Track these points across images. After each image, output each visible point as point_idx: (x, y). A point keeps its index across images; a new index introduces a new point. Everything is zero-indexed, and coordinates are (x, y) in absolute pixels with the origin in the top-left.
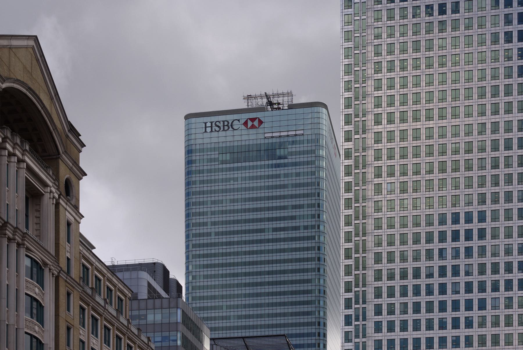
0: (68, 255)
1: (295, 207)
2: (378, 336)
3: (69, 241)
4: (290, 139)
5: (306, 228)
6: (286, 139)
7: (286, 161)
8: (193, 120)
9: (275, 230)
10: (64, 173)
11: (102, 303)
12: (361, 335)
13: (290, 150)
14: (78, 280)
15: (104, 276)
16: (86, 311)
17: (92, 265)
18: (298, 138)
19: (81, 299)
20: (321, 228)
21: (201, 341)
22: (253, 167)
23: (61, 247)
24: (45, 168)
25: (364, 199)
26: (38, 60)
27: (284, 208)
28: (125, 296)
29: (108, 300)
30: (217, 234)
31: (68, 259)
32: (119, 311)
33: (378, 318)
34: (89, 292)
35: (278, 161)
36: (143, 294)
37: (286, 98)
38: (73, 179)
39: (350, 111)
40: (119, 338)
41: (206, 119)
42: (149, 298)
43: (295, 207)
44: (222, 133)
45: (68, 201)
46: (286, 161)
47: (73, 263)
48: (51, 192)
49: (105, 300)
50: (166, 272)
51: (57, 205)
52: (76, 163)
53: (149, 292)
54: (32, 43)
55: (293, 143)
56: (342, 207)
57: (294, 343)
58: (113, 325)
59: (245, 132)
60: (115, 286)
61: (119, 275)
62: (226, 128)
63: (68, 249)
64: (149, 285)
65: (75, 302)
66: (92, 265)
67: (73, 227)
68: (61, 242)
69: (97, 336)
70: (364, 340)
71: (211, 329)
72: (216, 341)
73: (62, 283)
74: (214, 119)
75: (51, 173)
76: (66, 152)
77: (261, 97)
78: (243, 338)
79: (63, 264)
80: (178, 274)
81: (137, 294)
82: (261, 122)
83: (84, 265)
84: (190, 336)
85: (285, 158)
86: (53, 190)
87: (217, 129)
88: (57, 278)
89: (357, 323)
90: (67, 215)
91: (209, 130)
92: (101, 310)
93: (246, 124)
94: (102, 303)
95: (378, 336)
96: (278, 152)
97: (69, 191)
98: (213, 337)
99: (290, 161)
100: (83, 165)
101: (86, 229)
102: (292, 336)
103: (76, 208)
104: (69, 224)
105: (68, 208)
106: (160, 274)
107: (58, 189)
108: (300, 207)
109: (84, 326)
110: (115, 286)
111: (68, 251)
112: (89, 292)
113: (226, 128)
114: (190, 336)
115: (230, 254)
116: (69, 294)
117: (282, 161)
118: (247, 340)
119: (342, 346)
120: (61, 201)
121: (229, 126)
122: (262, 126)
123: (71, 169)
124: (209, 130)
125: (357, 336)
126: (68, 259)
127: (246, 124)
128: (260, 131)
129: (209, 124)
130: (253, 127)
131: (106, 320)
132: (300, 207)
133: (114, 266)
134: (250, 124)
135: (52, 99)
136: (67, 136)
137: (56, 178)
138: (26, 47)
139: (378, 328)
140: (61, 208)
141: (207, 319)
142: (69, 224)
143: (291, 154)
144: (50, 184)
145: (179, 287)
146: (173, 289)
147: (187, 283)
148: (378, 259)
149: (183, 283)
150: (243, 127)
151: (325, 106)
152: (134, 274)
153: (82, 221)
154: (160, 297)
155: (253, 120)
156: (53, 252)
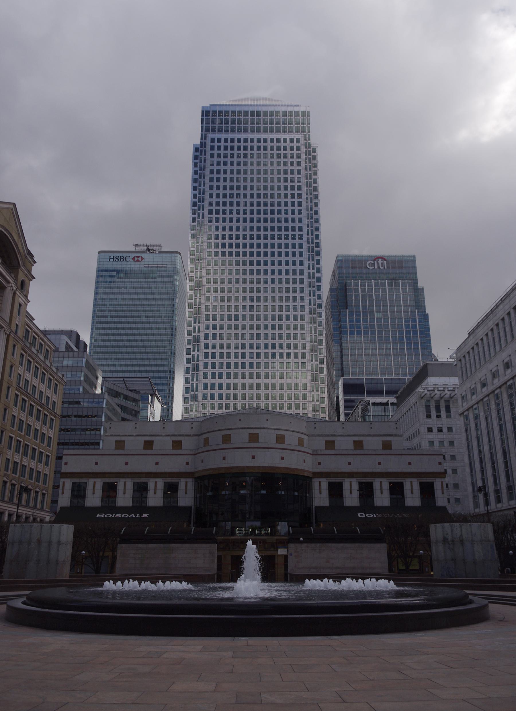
0: (17, 323)
1: (159, 305)
2: (206, 381)
3: (19, 315)
4: (159, 269)
5: (165, 317)
6: (156, 269)
7: (156, 280)
8: (103, 254)
9: (147, 317)
10: (21, 277)
11: (36, 352)
12: (195, 379)
13: (158, 274)
14: (21, 338)
15: (39, 336)
16: (25, 356)
17: (31, 329)
18: (163, 269)
19: (22, 349)
20: (174, 317)
21: (96, 378)
22: (136, 282)
23: (13, 318)
24: (10, 273)
25: (200, 304)
26: (14, 216)
27: (153, 305)
28: (51, 349)
29: (40, 350)
30: (112, 317)
31: (17, 325)
32: (46, 357)
33: (206, 370)
34: (28, 345)
35: (151, 280)
36: (63, 348)
37: (157, 248)
38: (27, 280)
39: (194, 257)
40: (44, 374)
41: (110, 254)
42: (66, 351)
43: (159, 305)
44: (119, 263)
45: (22, 292)
46: (156, 280)
47: (20, 327)
48: (11, 286)
49: (38, 351)
50: (78, 336)
51: (14, 294)
52: (29, 272)
53: (66, 348)
54: (12, 206)
55: (160, 271)
56: (187, 307)
57: (154, 382)
58: (41, 366)
59: (133, 263)
60: (45, 343)
61: (49, 336)
62: (122, 260)
63: (18, 319)
64: (67, 343)
65: (18, 351)
66: (31, 329)
67: (22, 307)
68: (14, 315)
69: (29, 372)
70: (197, 382)
71: (103, 371)
72: (106, 379)
73: (11, 339)
74: (115, 255)
75: (13, 276)
76: (24, 265)
77: (144, 246)
78: (123, 378)
79: (13, 328)
80: (86, 337)
81: (58, 348)
82: (142, 259)
83: (26, 329)
84: (89, 375)
85: (155, 278)
86: (13, 285)
87: (117, 260)
88: (8, 336)
89: (193, 372)
90: (20, 299)
91: (112, 260)
92: (34, 357)
93: (133, 259)
94: (36, 352)
95: (206, 381)
96: (151, 275)
97: (23, 286)
98: (104, 376)
99: (158, 280)
100: (33, 273)
101: (30, 309)
102: (153, 378)
103: (26, 296)
104: (20, 305)
105: (21, 296)
106: (74, 338)
107: (16, 285)
108: (163, 305)
109: (22, 365)
110: (45, 343)
111: (17, 320)
112: (28, 345)
113: (122, 260)
114: (89, 375)
115: (119, 329)
116: (14, 346)
117: (153, 280)
118: (125, 379)
119: (184, 386)
120: (17, 292)
121: (123, 259)
122: (143, 260)
123: (26, 275)
124: (112, 260)
125: (193, 380)
126: (17, 325)
127: (133, 259)
128: (142, 263)
129: (112, 257)
130: (138, 261)
131: (37, 362)
132: (163, 305)
133: (46, 331)
134: (136, 259)
135: (19, 236)
136: (26, 257)
137: (16, 279)
138: (8, 209)
139: (205, 376)
140: (16, 295)
141: (101, 365)
142: (20, 305)
143: (159, 276)
144: (12, 282)
145: (86, 346)
146: (82, 346)
147: (91, 343)
148: (207, 336)
149: (88, 343)
150: (132, 260)
151: (180, 254)
152: (58, 337)
153: (29, 304)
154: (73, 350)
155: (138, 257)
156: (8, 320)
